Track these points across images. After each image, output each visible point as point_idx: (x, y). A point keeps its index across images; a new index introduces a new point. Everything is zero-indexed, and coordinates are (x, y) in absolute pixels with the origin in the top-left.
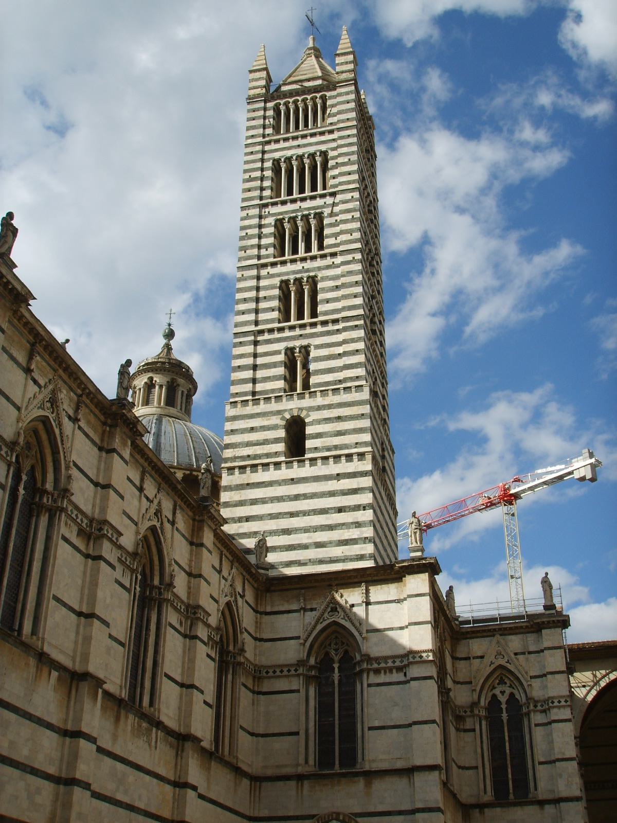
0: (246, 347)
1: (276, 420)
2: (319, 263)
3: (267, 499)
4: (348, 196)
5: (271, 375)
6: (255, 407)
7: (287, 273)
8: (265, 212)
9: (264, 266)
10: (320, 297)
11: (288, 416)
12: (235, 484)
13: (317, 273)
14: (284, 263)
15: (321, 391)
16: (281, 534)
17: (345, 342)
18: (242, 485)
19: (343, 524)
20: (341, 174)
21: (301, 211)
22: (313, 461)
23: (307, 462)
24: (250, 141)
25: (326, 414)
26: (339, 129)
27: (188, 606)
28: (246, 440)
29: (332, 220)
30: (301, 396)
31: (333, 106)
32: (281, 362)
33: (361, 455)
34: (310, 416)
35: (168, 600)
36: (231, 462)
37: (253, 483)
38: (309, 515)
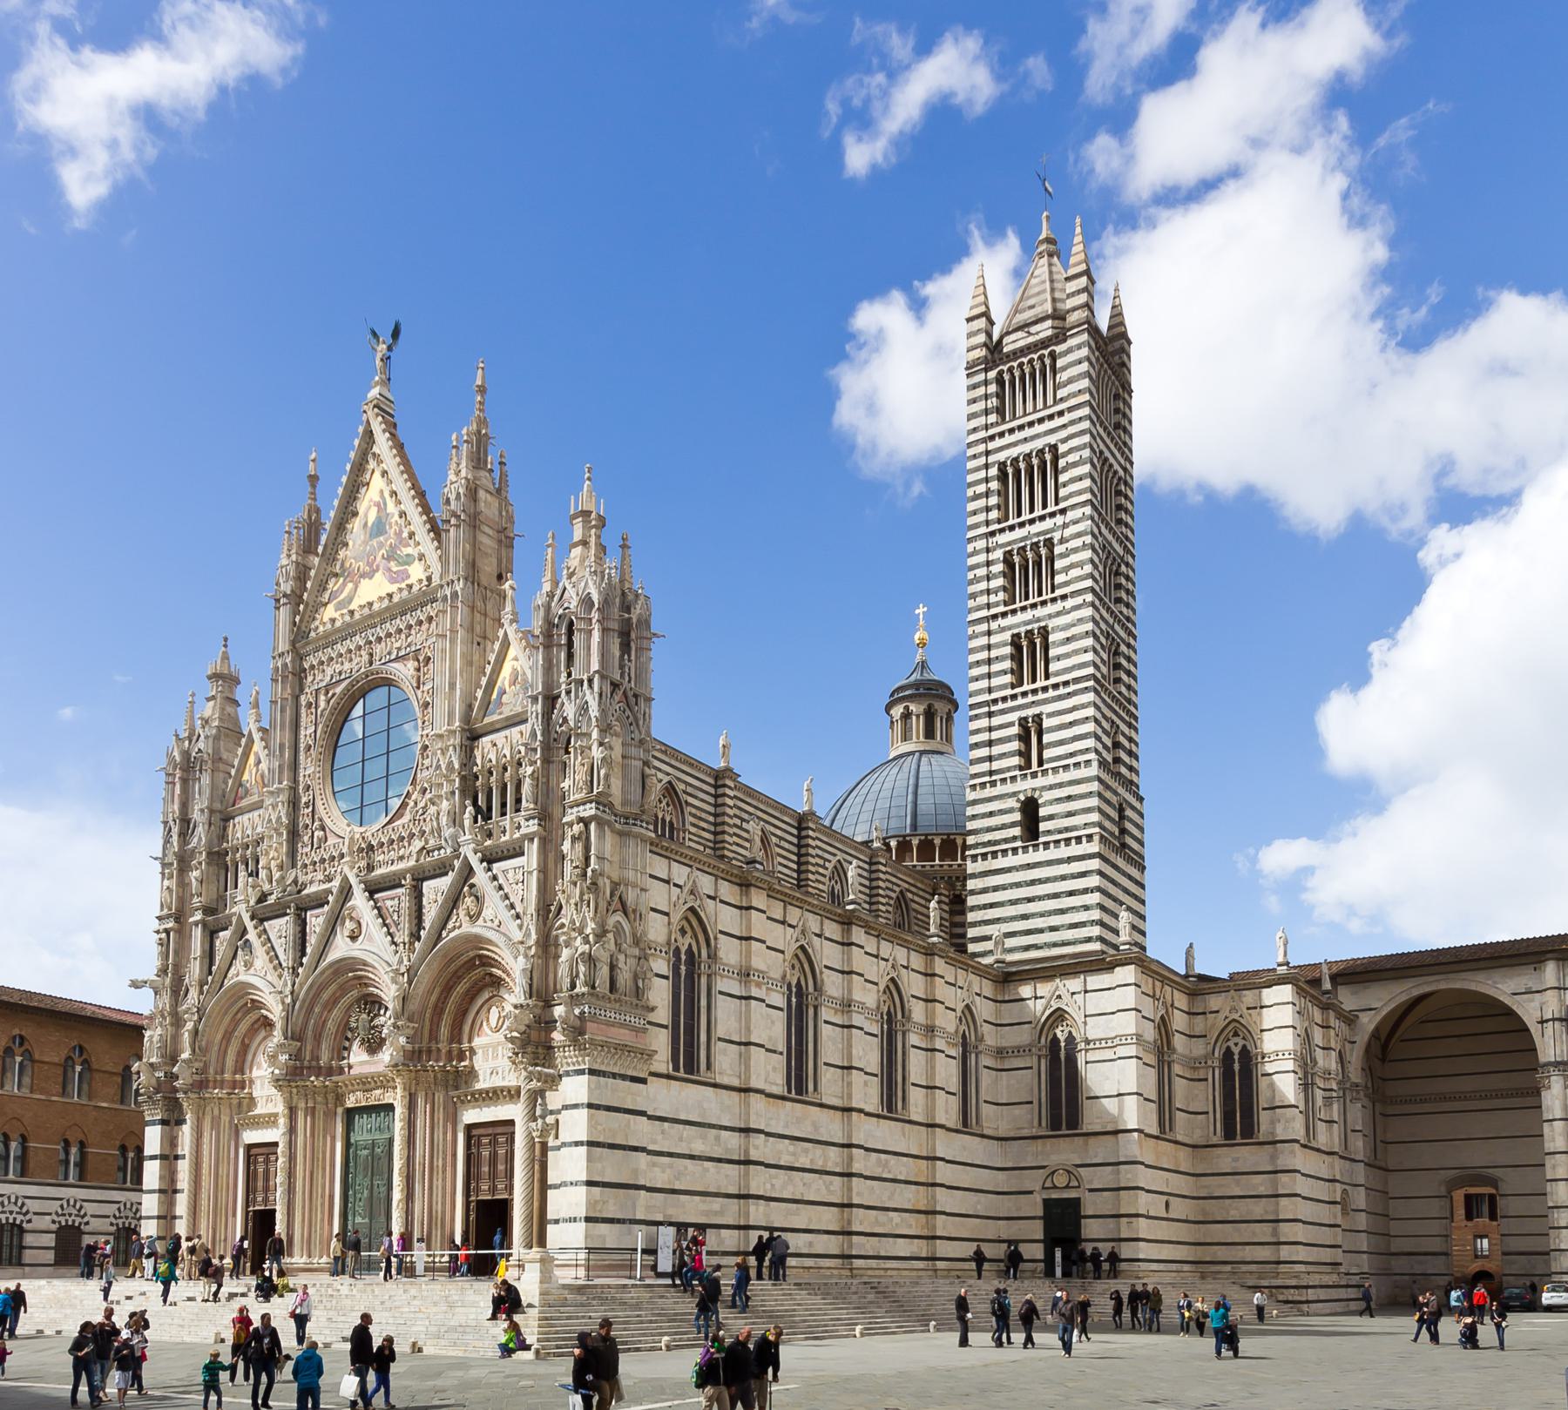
7: (1018, 625)
9: (995, 617)
10: (1052, 652)
17: (1074, 709)
27: (927, 1027)
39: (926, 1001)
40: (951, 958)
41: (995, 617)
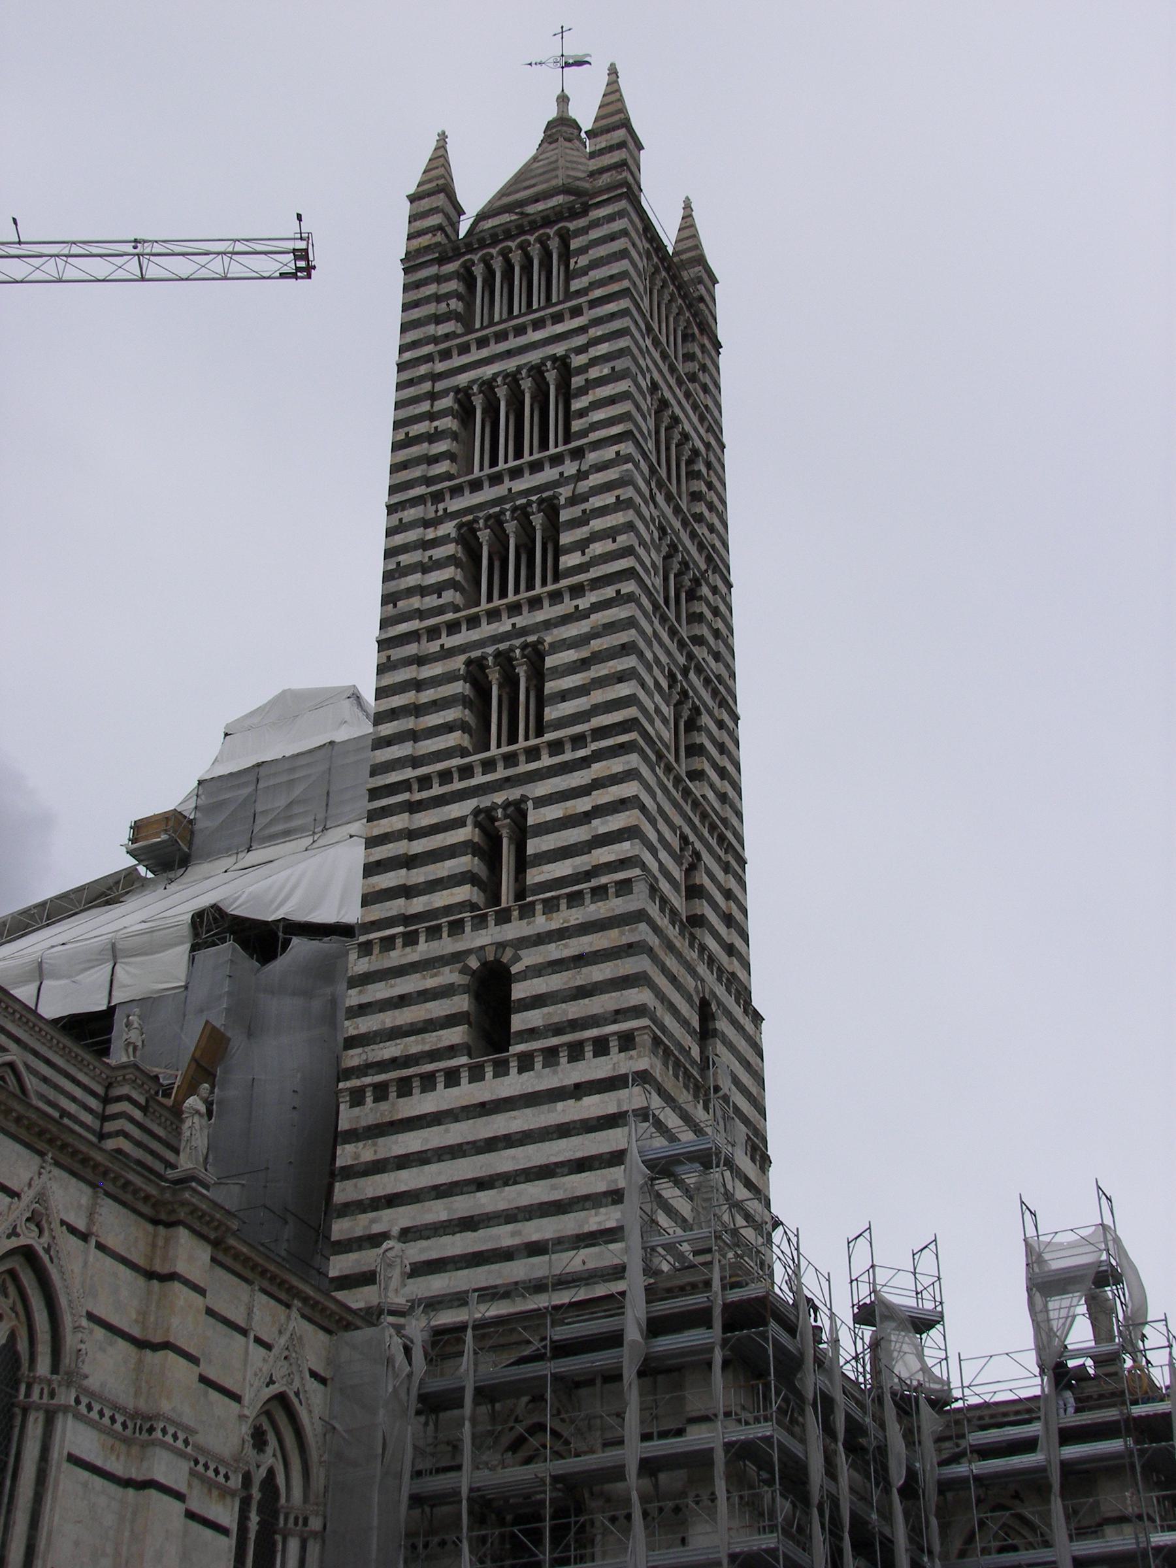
0: (394, 818)
1: (449, 976)
2: (548, 612)
3: (429, 1154)
4: (609, 453)
5: (445, 874)
6: (408, 949)
7: (481, 644)
8: (437, 511)
10: (551, 687)
11: (474, 963)
12: (364, 1123)
13: (541, 634)
14: (473, 622)
15: (544, 901)
16: (457, 1229)
18: (377, 1126)
19: (587, 1198)
20: (596, 405)
21: (513, 500)
22: (526, 1063)
23: (513, 1064)
24: (408, 355)
25: (554, 951)
26: (593, 304)
27: (135, 1415)
28: (389, 1024)
29: (575, 512)
30: (504, 917)
31: (583, 250)
32: (466, 844)
33: (627, 1041)
34: (518, 959)
35: (65, 1409)
36: (358, 1078)
37: (401, 1120)
38: (515, 1183)
39: (141, 1344)
40: (237, 1256)
41: (433, 633)
